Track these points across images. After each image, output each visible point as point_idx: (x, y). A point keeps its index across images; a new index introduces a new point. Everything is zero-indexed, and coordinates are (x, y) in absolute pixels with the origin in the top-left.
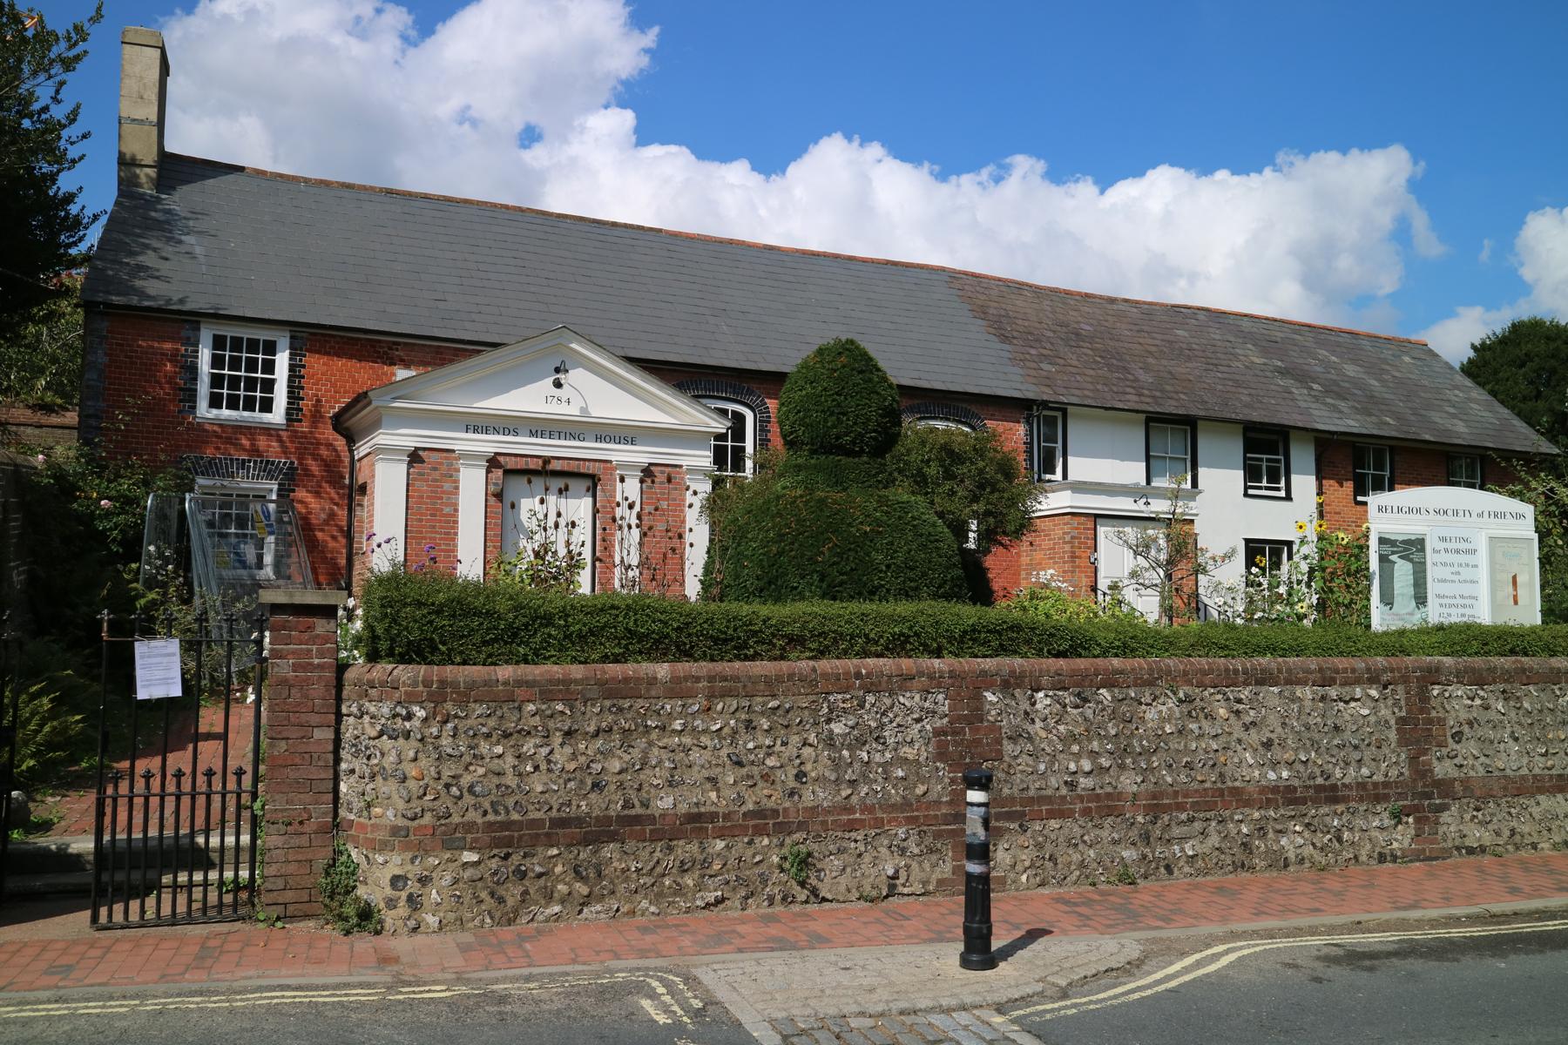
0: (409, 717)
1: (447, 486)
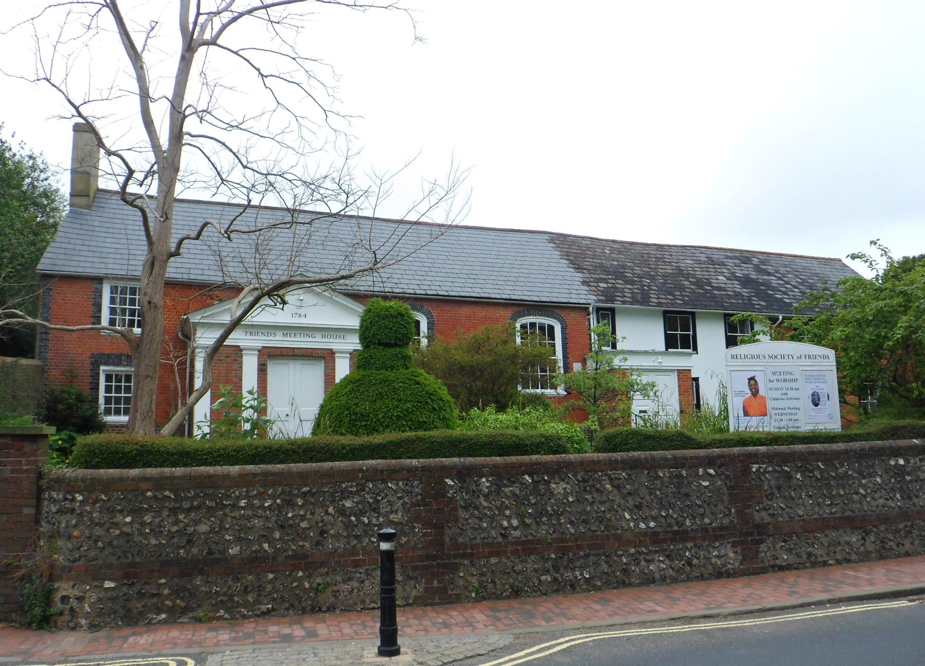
0: (74, 499)
1: (235, 366)
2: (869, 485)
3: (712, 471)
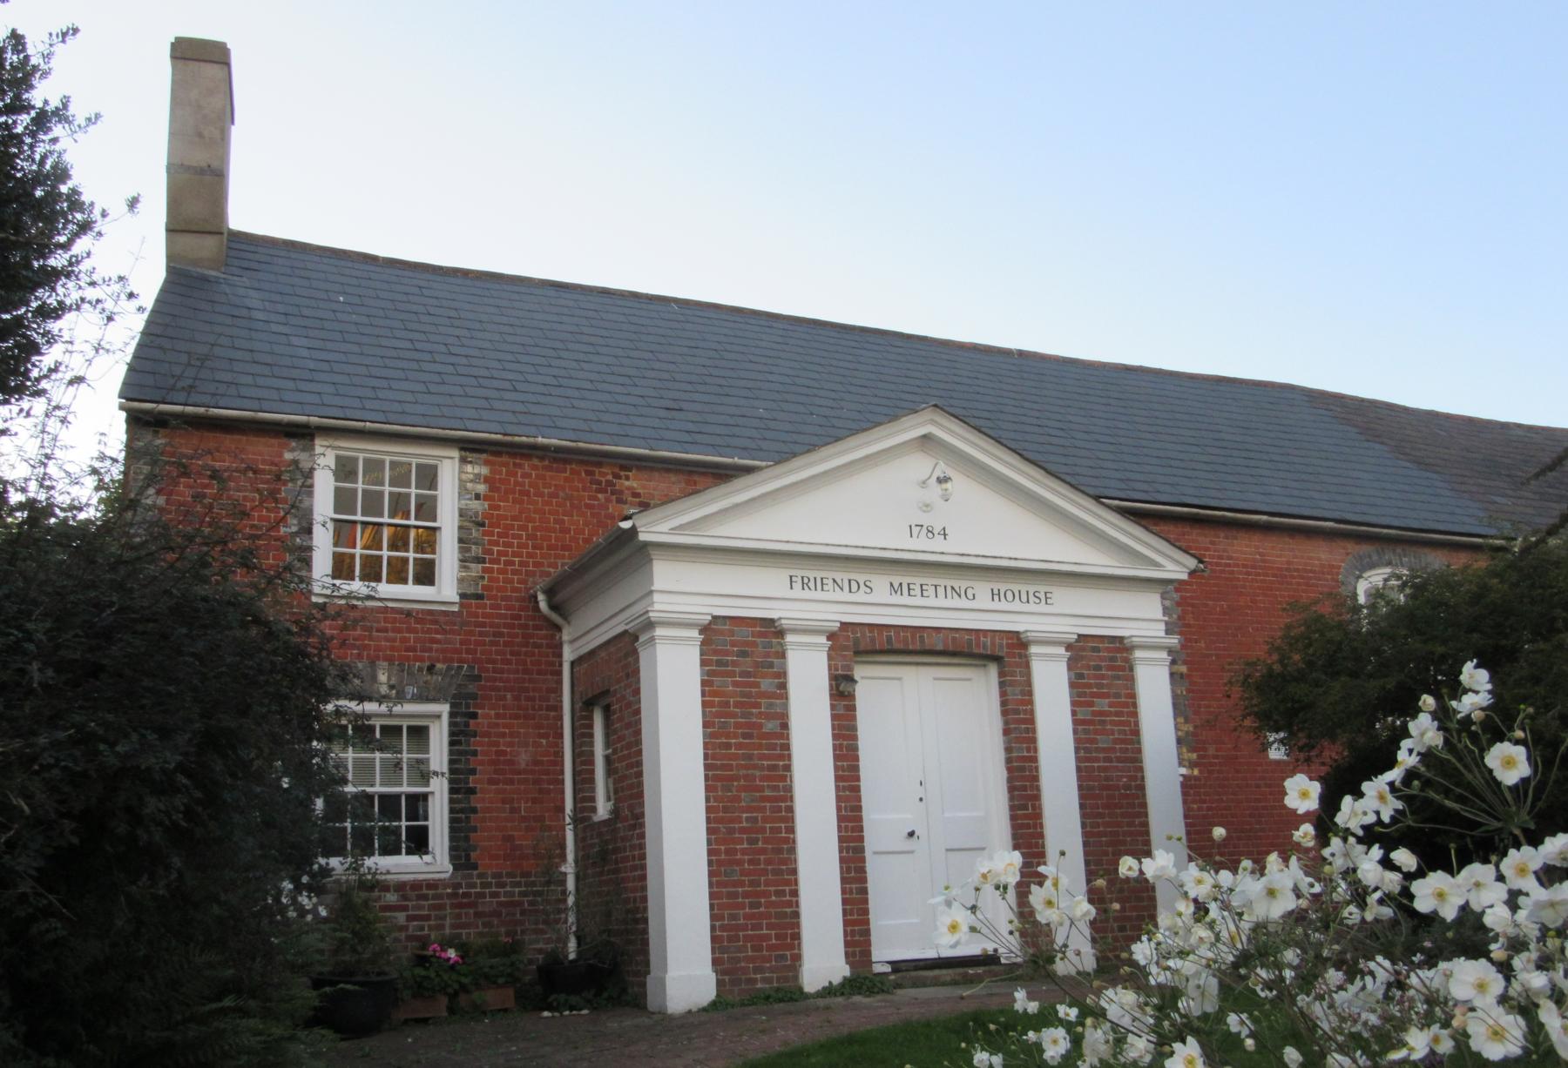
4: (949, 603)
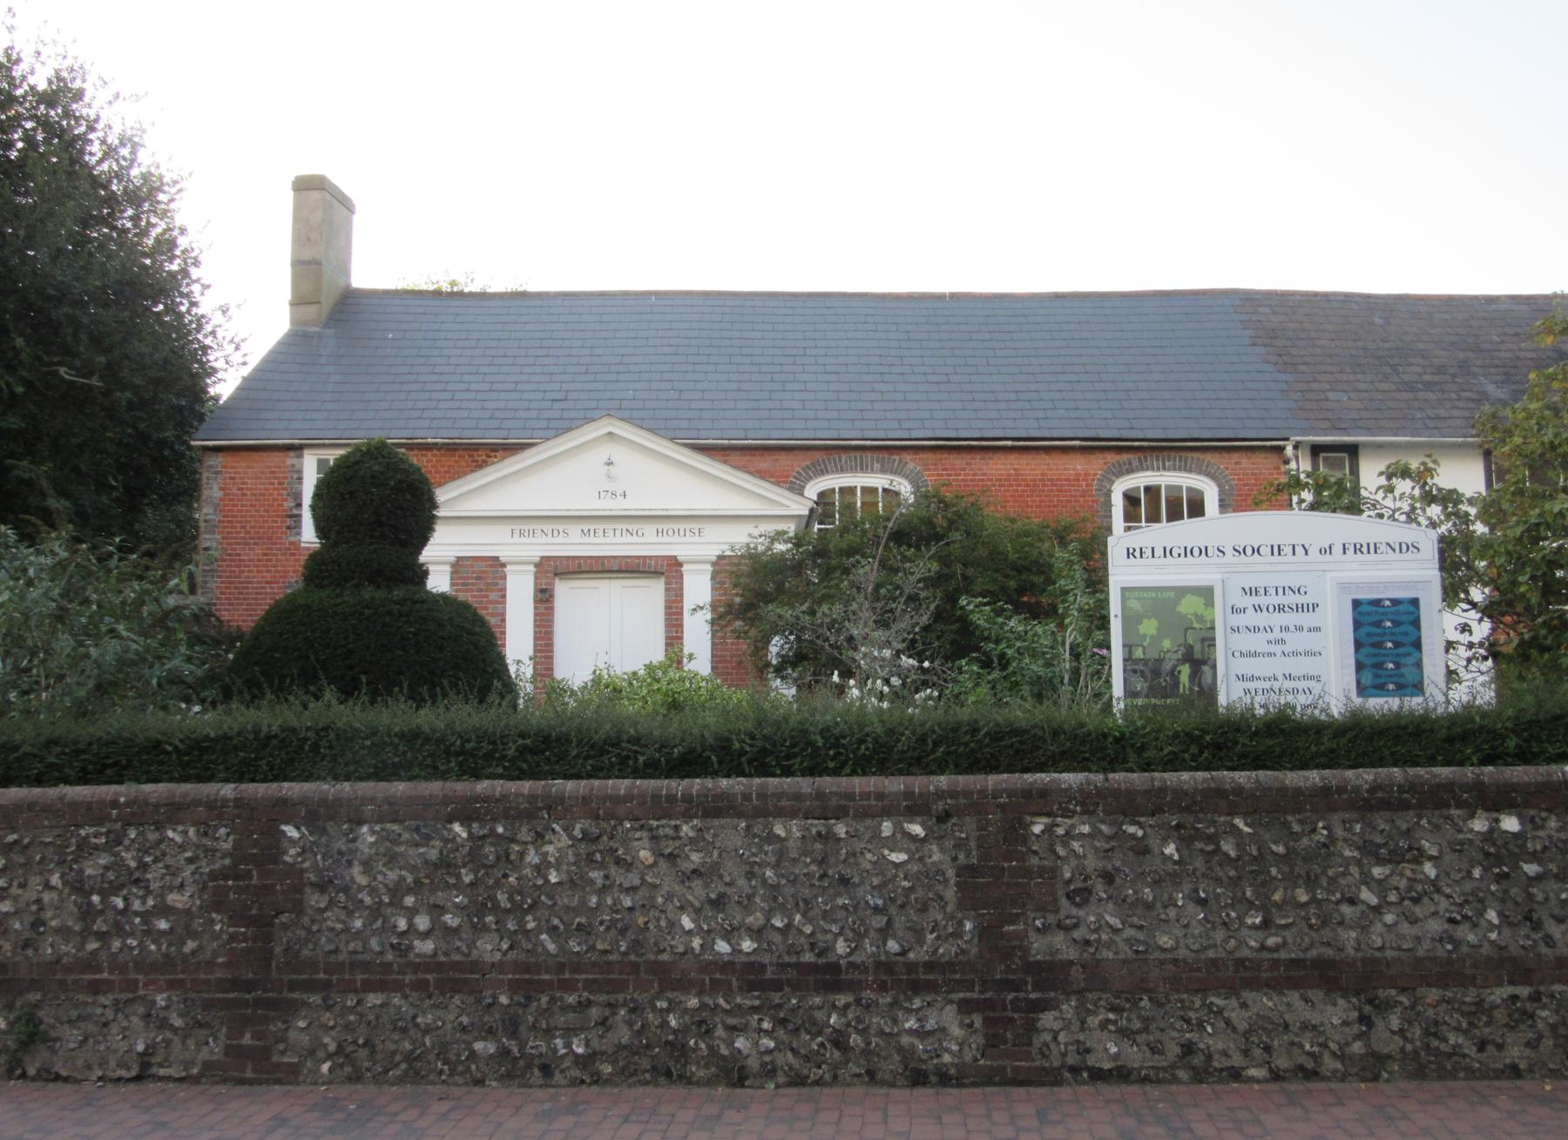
1: (493, 596)
2: (1395, 880)
3: (917, 829)
4: (618, 539)
